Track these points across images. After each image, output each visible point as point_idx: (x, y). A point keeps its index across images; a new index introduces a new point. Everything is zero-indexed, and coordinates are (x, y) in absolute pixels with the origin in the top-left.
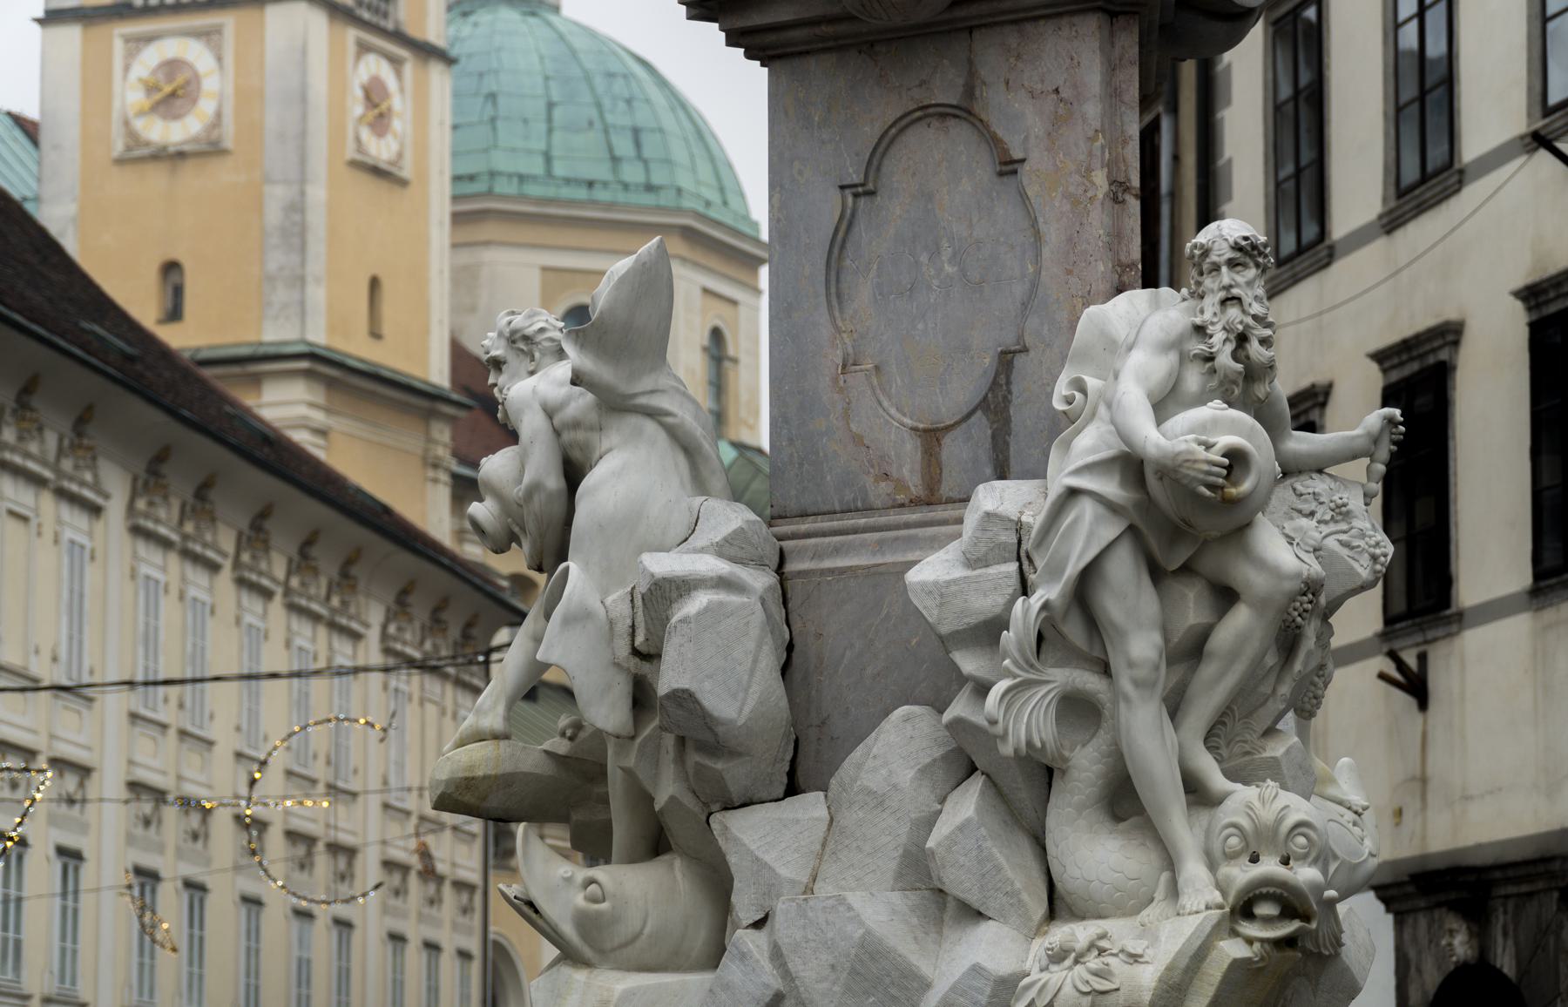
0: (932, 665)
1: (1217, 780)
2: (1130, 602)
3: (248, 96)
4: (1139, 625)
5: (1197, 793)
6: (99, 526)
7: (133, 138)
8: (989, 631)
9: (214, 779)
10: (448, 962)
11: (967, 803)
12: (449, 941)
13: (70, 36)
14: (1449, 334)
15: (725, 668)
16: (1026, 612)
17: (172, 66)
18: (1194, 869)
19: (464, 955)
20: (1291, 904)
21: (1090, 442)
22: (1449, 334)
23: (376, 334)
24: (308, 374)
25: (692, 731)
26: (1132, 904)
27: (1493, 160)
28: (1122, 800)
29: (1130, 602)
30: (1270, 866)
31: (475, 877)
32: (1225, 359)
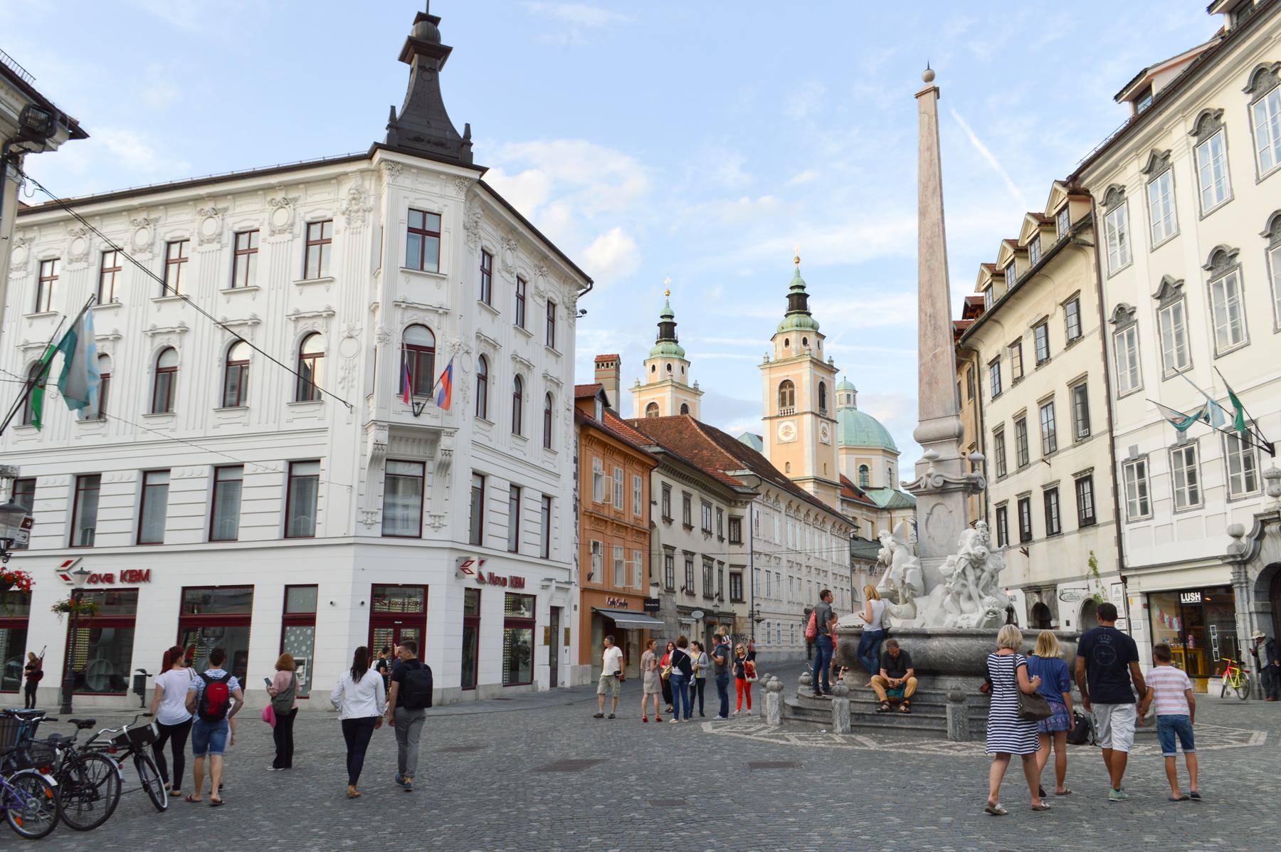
0: (943, 579)
2: (970, 572)
3: (800, 431)
4: (971, 575)
5: (980, 597)
8: (951, 576)
9: (801, 559)
11: (949, 597)
15: (914, 579)
17: (787, 427)
21: (962, 552)
22: (1030, 492)
25: (910, 587)
26: (972, 612)
27: (1035, 463)
28: (970, 598)
29: (970, 572)
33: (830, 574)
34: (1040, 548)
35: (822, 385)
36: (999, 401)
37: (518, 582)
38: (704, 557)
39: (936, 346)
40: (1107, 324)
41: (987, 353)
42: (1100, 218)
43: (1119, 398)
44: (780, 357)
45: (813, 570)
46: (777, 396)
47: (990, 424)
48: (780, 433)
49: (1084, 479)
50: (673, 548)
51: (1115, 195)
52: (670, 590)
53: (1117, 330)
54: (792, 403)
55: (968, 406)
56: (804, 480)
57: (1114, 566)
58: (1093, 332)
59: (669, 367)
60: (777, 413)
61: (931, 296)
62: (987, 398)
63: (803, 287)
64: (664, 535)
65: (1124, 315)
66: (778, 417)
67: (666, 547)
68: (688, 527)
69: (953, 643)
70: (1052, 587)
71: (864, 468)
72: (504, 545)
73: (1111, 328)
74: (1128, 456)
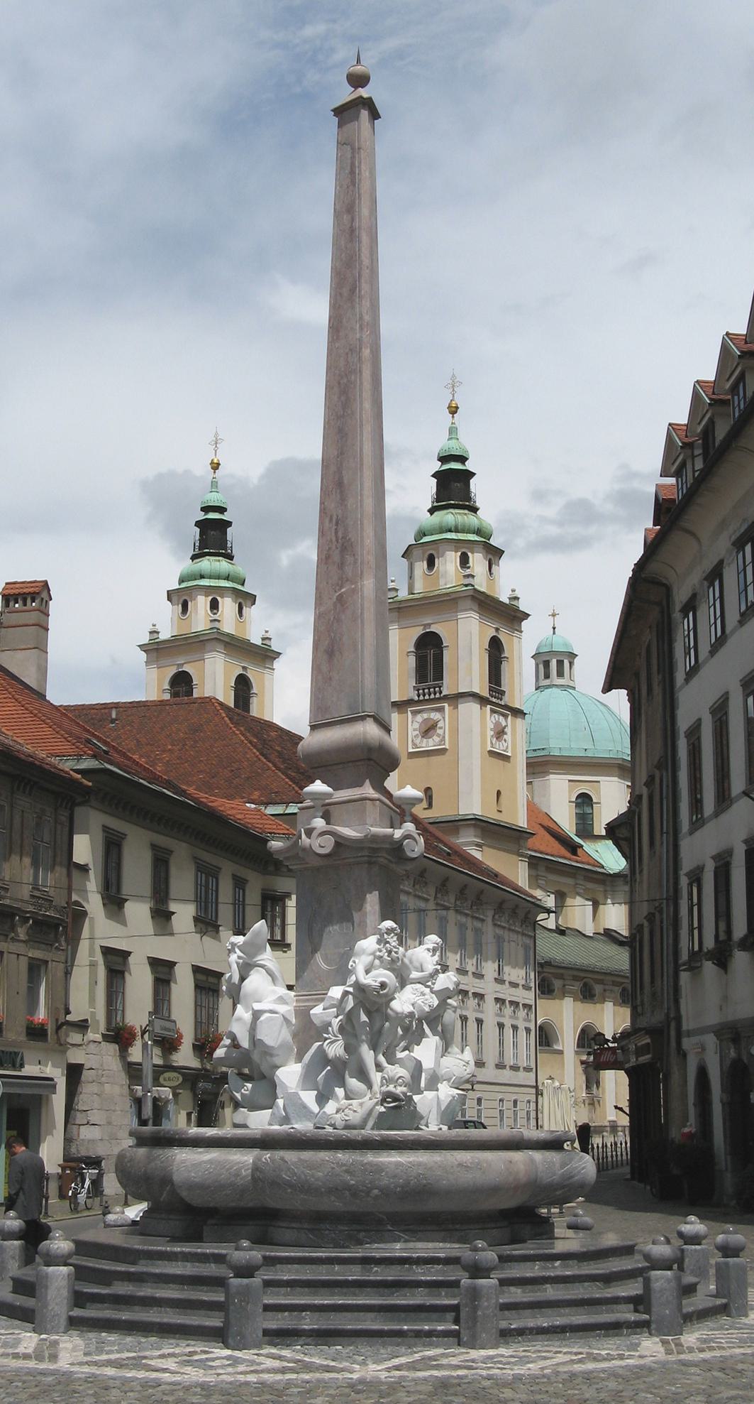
1: (385, 1064)
10: (522, 1034)
12: (522, 1025)
16: (336, 1022)
18: (376, 1087)
20: (395, 1098)
24: (474, 826)
30: (391, 1088)
33: (489, 1000)
36: (695, 681)
38: (197, 970)
39: (342, 581)
41: (681, 596)
44: (419, 587)
46: (412, 661)
47: (683, 724)
54: (439, 675)
55: (657, 690)
56: (456, 824)
59: (214, 605)
61: (340, 484)
62: (680, 676)
63: (462, 459)
67: (107, 951)
69: (291, 1156)
71: (584, 801)
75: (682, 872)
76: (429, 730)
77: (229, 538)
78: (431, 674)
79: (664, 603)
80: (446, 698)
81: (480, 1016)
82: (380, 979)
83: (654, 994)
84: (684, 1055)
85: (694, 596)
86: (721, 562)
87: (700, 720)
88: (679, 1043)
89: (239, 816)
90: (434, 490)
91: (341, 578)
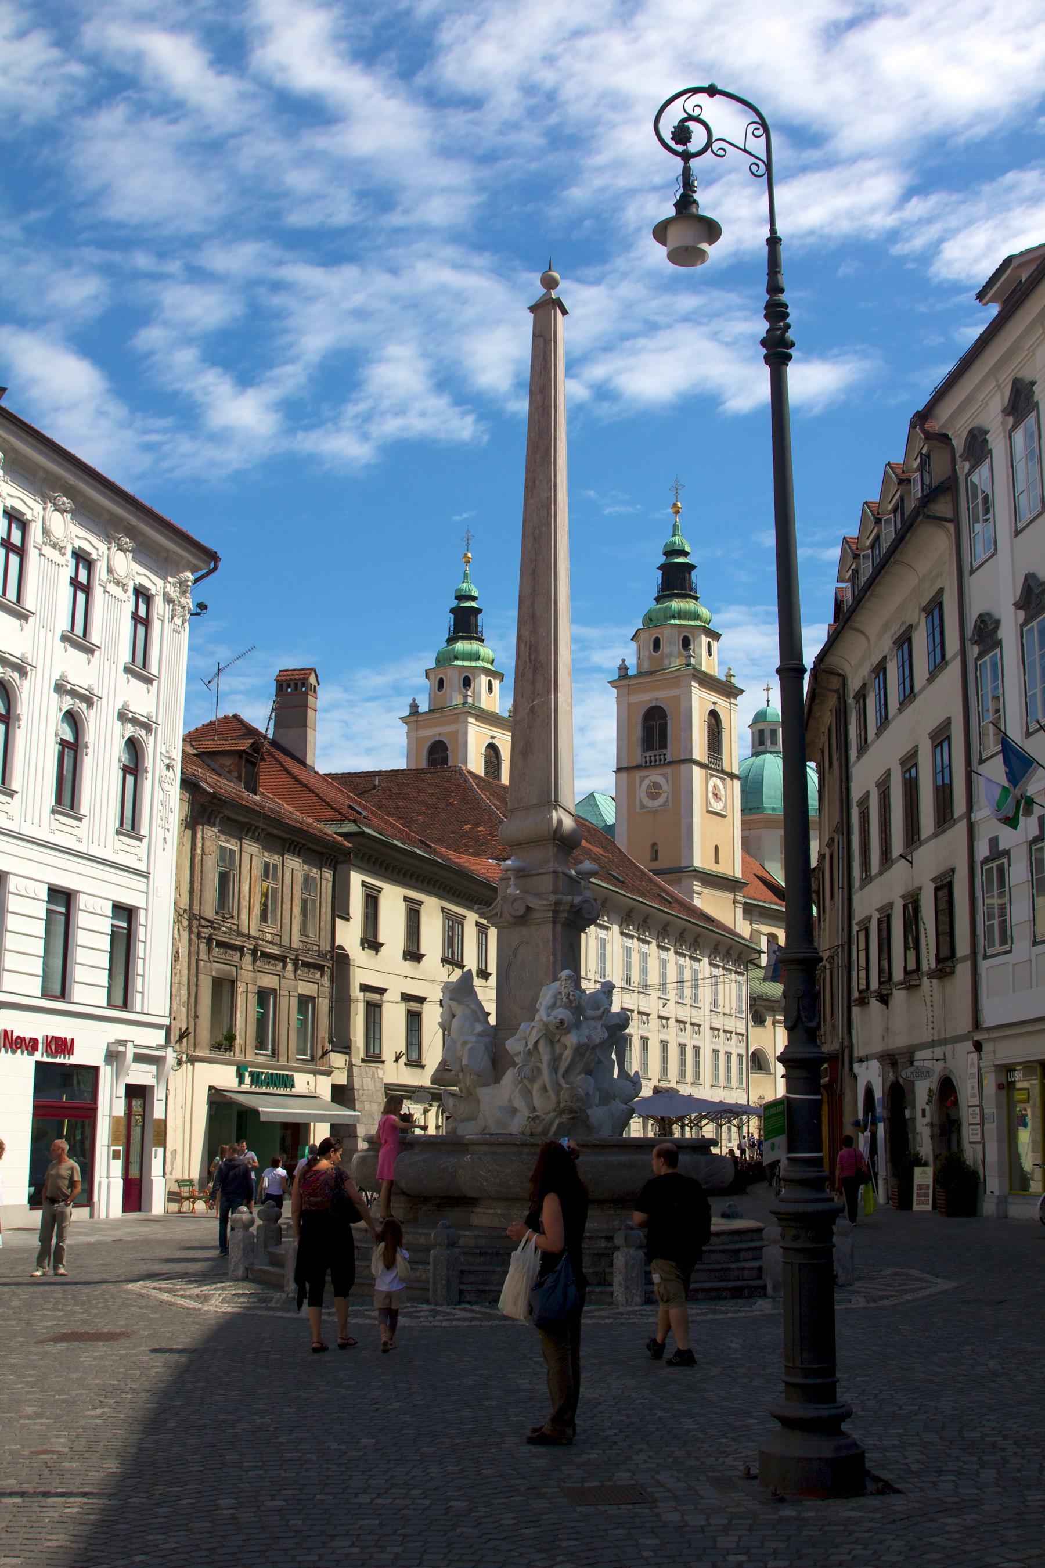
6: (610, 932)
7: (643, 806)
13: (624, 775)
14: (891, 905)
19: (740, 1056)
20: (571, 1111)
22: (891, 905)
23: (717, 862)
31: (744, 1031)
32: (565, 999)
33: (705, 1029)
34: (899, 996)
35: (714, 714)
36: (865, 758)
37: (62, 1045)
40: (968, 644)
41: (854, 685)
42: (962, 478)
43: (981, 761)
44: (646, 667)
45: (672, 1022)
46: (638, 732)
48: (642, 793)
49: (944, 887)
50: (382, 991)
51: (977, 446)
52: (373, 1057)
53: (981, 655)
54: (663, 745)
55: (836, 764)
57: (964, 1024)
58: (954, 657)
60: (638, 758)
61: (533, 616)
62: (853, 753)
64: (365, 967)
65: (986, 632)
66: (638, 767)
67: (365, 988)
68: (413, 954)
70: (909, 1055)
72: (35, 987)
73: (974, 651)
74: (988, 854)
75: (854, 922)
76: (654, 791)
77: (480, 623)
78: (656, 744)
79: (841, 691)
80: (670, 763)
81: (697, 1044)
82: (560, 1017)
83: (833, 1025)
84: (856, 1078)
85: (864, 685)
86: (885, 657)
87: (868, 792)
88: (851, 1069)
89: (482, 871)
90: (660, 581)
91: (533, 693)
